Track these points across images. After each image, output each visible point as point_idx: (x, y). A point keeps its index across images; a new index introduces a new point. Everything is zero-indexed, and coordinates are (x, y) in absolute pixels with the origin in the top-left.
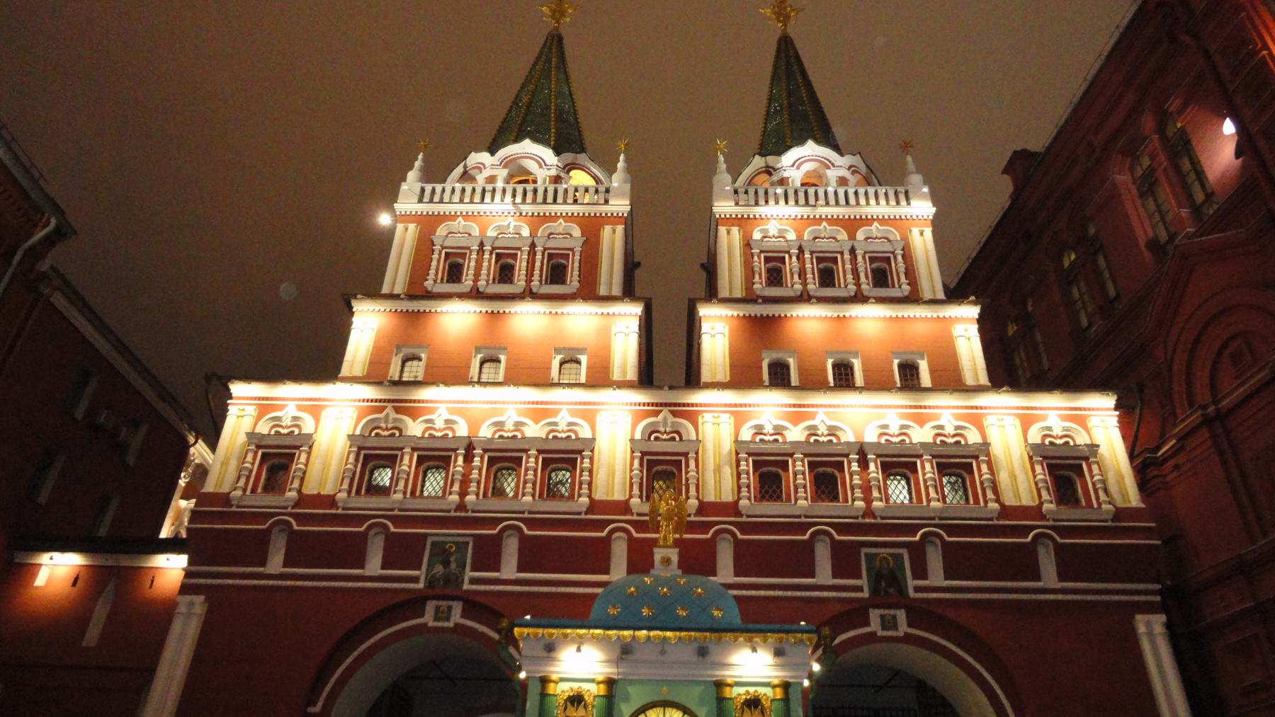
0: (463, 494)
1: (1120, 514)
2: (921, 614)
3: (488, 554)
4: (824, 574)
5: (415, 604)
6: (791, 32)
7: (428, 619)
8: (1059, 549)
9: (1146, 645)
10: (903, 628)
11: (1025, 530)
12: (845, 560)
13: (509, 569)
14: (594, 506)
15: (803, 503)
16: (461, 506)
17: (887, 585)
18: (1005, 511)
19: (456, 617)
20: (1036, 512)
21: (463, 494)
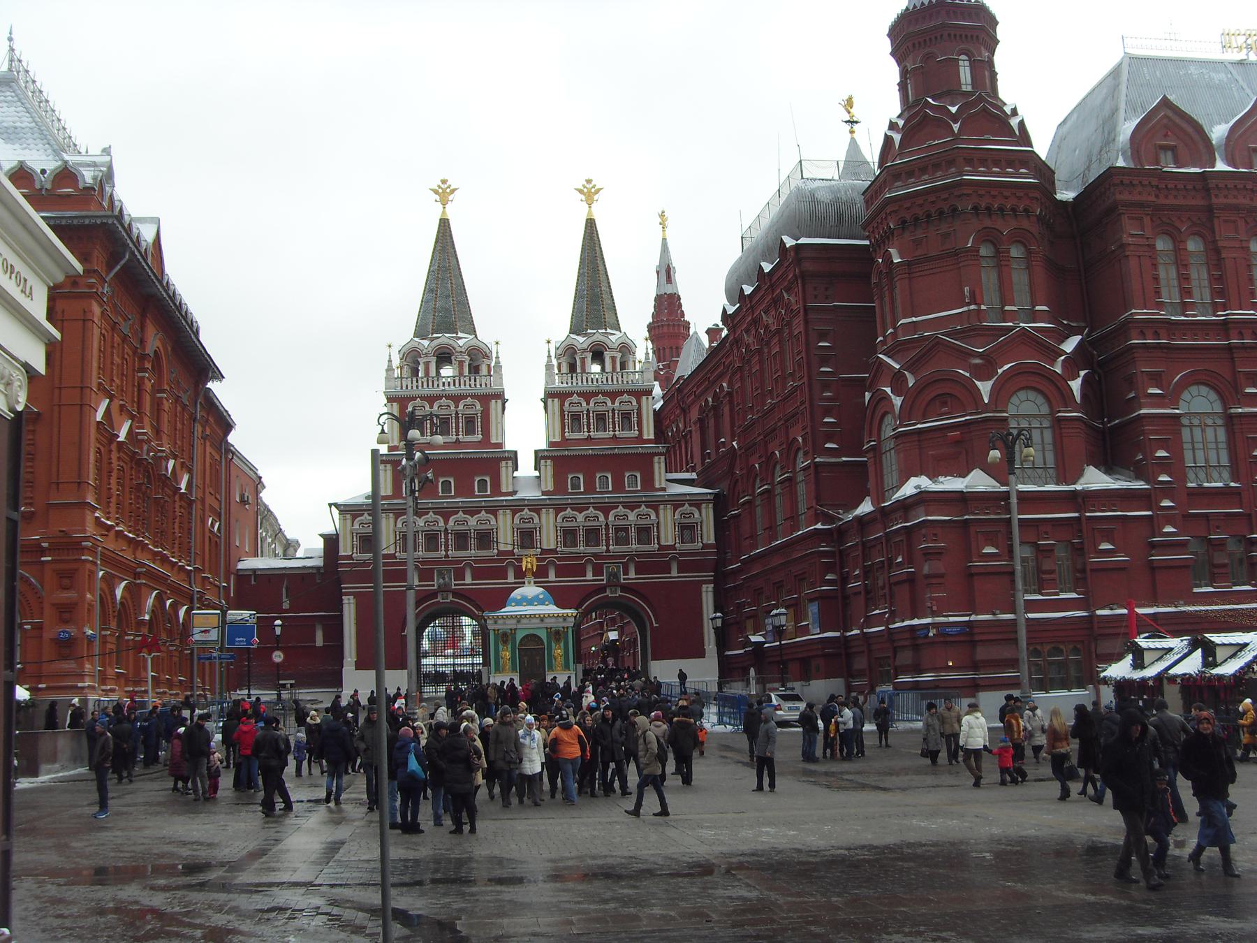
0: (447, 550)
1: (705, 546)
2: (625, 588)
3: (460, 575)
4: (589, 576)
5: (434, 594)
6: (595, 217)
7: (439, 599)
8: (679, 562)
9: (704, 594)
10: (619, 593)
11: (666, 555)
12: (598, 571)
13: (468, 580)
14: (500, 553)
15: (582, 548)
16: (447, 556)
17: (613, 581)
18: (661, 547)
19: (450, 598)
20: (673, 547)
21: (447, 550)
